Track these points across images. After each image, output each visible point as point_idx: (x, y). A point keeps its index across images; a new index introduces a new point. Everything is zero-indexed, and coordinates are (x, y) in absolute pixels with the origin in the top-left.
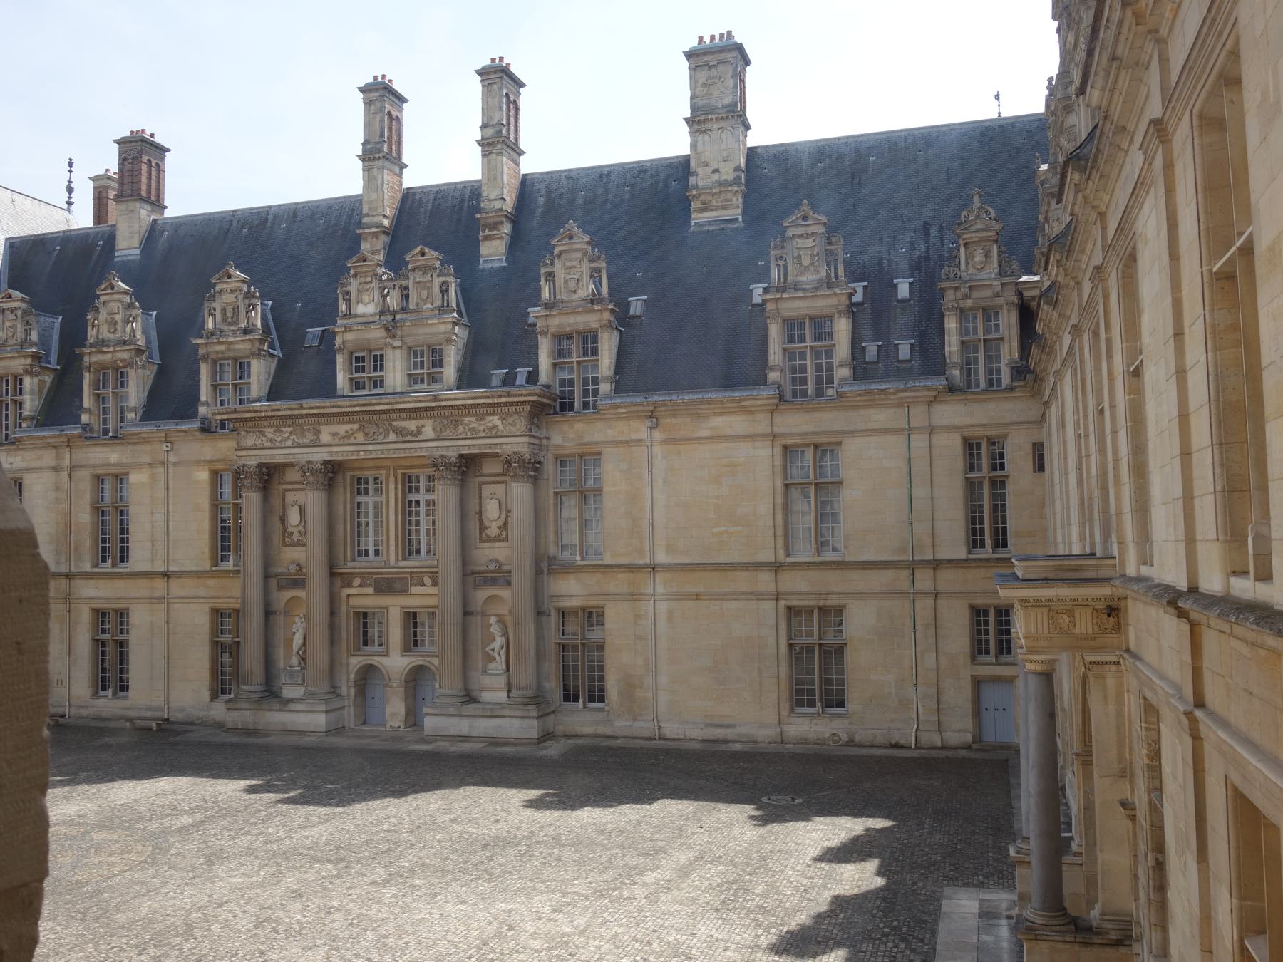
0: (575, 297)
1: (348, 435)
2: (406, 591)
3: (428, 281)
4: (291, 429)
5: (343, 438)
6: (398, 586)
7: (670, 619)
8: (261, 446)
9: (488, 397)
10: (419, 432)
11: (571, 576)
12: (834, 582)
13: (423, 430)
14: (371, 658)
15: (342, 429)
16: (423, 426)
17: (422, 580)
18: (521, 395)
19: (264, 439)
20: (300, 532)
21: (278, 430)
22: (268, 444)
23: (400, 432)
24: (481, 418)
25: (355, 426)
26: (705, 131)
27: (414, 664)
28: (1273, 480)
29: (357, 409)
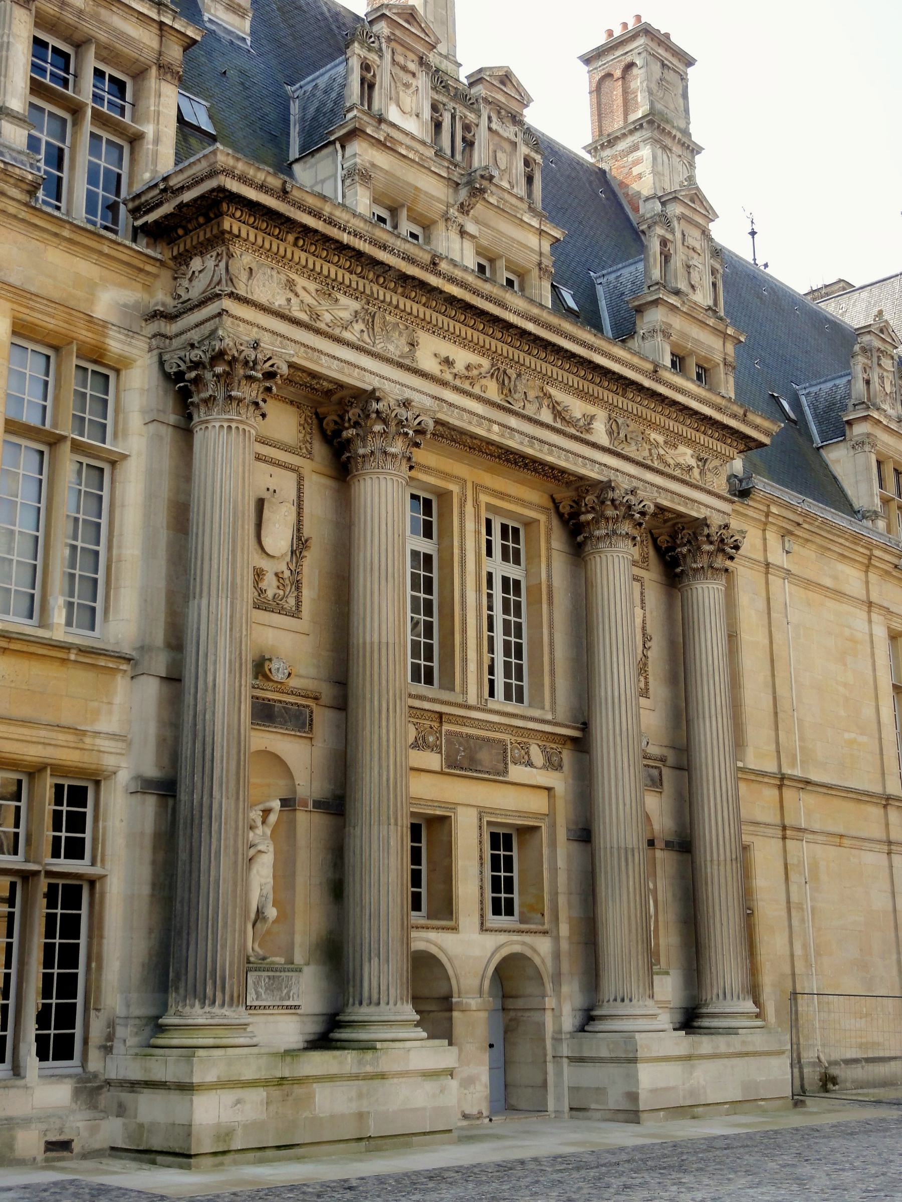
1: (470, 374)
2: (505, 772)
6: (485, 756)
17: (527, 753)
22: (303, 317)
25: (486, 363)
26: (665, 148)
27: (505, 952)
28: (885, 791)
29: (530, 327)
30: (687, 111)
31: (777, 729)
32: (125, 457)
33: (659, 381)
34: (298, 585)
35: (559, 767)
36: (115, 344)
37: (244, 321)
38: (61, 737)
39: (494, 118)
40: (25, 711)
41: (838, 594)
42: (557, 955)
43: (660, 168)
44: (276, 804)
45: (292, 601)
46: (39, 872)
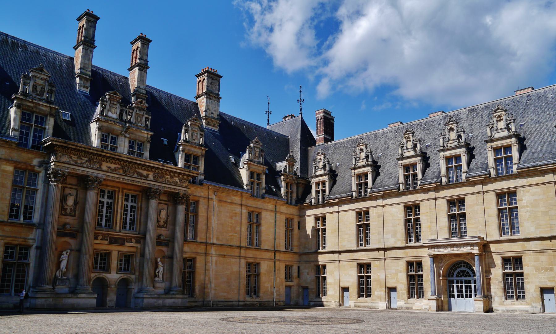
0: (194, 142)
1: (115, 170)
2: (124, 244)
3: (141, 114)
4: (86, 159)
5: (113, 170)
7: (216, 264)
8: (69, 163)
9: (182, 170)
10: (147, 176)
11: (186, 245)
12: (258, 254)
13: (149, 176)
14: (102, 274)
15: (113, 166)
16: (149, 174)
17: (131, 240)
18: (194, 173)
19: (71, 160)
20: (71, 209)
21: (79, 157)
22: (73, 163)
23: (140, 175)
24: (172, 177)
25: (119, 167)
26: (210, 99)
27: (122, 278)
29: (129, 160)
30: (219, 89)
31: (207, 233)
32: (38, 189)
33: (165, 166)
34: (75, 210)
35: (140, 243)
36: (37, 169)
37: (59, 166)
38: (21, 240)
39: (137, 111)
40: (14, 235)
41: (232, 203)
42: (136, 278)
43: (208, 104)
44: (69, 251)
45: (73, 214)
46: (16, 262)
